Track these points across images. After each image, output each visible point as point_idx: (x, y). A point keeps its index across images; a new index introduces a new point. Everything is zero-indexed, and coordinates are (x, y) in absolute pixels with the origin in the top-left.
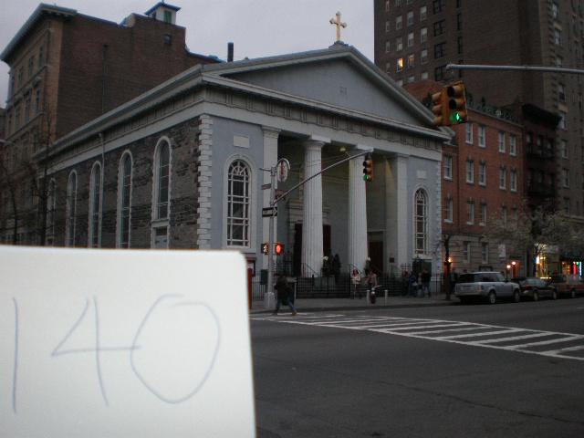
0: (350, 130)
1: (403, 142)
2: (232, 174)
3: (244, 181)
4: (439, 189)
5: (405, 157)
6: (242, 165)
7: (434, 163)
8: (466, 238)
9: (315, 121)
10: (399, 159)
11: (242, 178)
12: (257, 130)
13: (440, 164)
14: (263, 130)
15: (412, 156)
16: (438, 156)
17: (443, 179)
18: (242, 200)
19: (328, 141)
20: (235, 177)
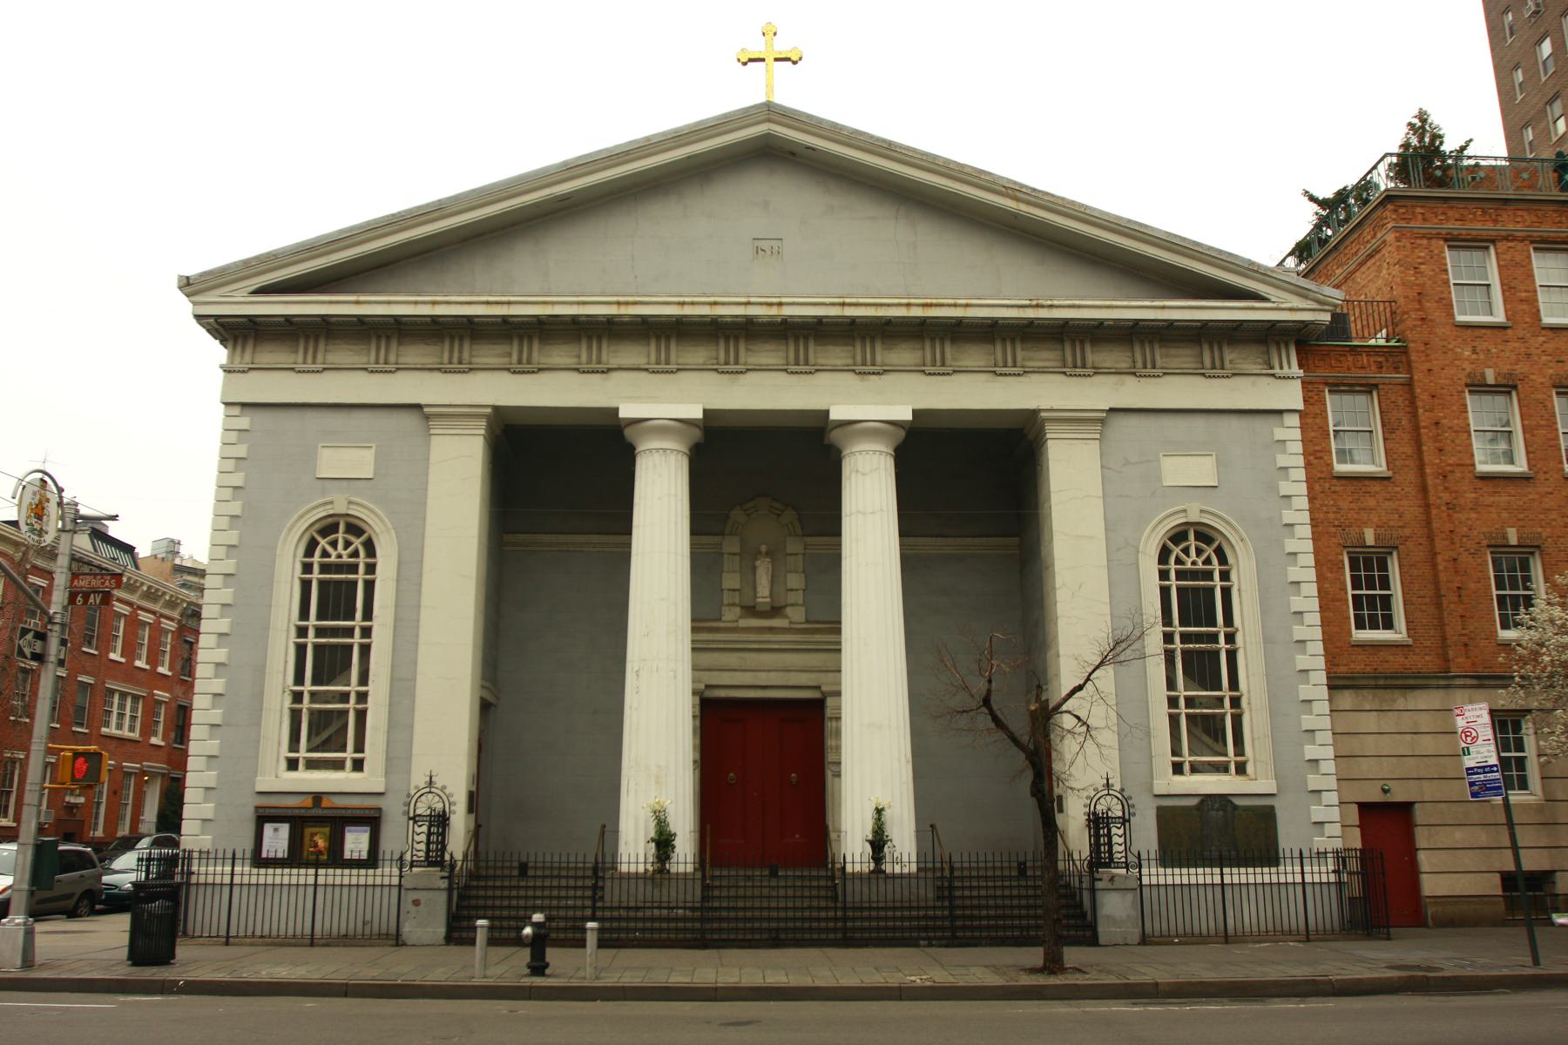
0: (801, 367)
1: (1078, 368)
2: (316, 559)
3: (361, 576)
4: (1299, 513)
5: (1076, 420)
6: (355, 529)
7: (1259, 423)
8: (1504, 699)
9: (641, 361)
10: (1048, 427)
11: (353, 568)
12: (409, 421)
13: (1294, 420)
14: (427, 417)
15: (1112, 410)
16: (1290, 395)
17: (1322, 481)
18: (320, 632)
19: (696, 413)
20: (325, 568)
